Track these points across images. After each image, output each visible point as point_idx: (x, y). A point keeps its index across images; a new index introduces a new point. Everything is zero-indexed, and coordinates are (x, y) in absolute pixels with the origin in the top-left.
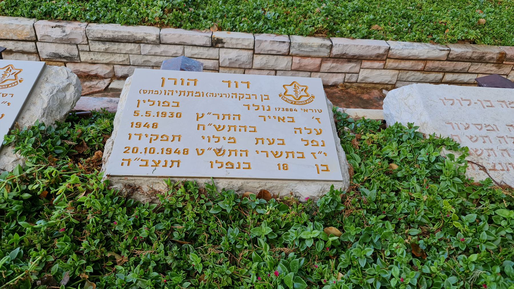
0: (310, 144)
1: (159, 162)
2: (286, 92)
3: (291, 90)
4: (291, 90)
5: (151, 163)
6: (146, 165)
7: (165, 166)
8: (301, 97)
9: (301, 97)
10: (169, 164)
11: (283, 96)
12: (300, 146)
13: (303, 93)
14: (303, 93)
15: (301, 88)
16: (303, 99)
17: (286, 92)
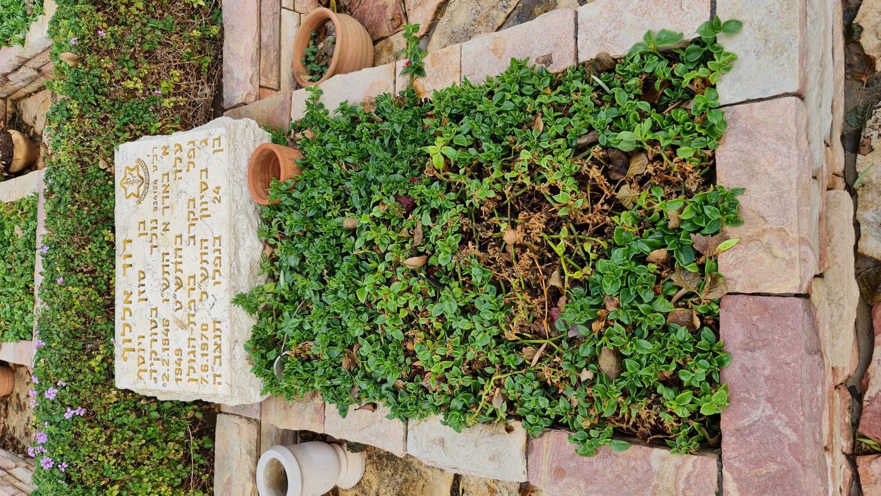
0: (192, 160)
1: (215, 344)
2: (134, 195)
3: (133, 189)
4: (133, 189)
5: (217, 354)
6: (220, 357)
7: (219, 336)
8: (140, 176)
9: (140, 176)
10: (218, 333)
11: (140, 198)
12: (195, 172)
13: (135, 173)
14: (135, 173)
15: (129, 176)
16: (142, 174)
17: (134, 195)
